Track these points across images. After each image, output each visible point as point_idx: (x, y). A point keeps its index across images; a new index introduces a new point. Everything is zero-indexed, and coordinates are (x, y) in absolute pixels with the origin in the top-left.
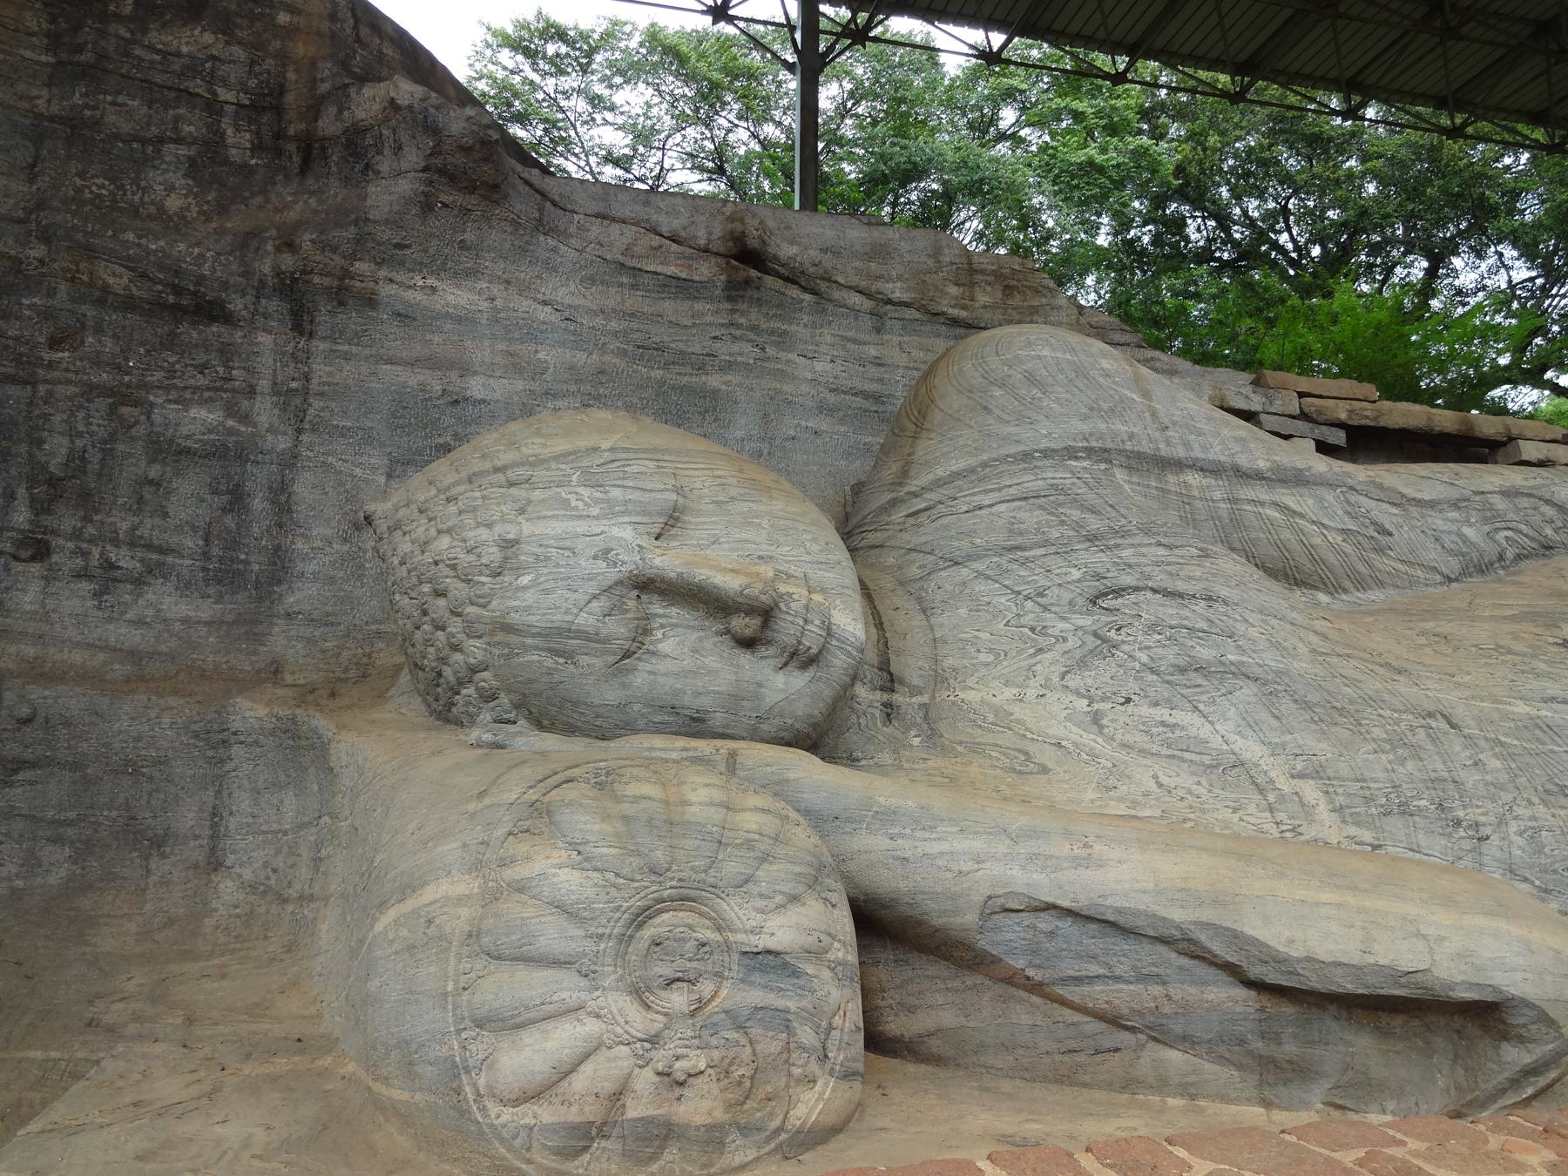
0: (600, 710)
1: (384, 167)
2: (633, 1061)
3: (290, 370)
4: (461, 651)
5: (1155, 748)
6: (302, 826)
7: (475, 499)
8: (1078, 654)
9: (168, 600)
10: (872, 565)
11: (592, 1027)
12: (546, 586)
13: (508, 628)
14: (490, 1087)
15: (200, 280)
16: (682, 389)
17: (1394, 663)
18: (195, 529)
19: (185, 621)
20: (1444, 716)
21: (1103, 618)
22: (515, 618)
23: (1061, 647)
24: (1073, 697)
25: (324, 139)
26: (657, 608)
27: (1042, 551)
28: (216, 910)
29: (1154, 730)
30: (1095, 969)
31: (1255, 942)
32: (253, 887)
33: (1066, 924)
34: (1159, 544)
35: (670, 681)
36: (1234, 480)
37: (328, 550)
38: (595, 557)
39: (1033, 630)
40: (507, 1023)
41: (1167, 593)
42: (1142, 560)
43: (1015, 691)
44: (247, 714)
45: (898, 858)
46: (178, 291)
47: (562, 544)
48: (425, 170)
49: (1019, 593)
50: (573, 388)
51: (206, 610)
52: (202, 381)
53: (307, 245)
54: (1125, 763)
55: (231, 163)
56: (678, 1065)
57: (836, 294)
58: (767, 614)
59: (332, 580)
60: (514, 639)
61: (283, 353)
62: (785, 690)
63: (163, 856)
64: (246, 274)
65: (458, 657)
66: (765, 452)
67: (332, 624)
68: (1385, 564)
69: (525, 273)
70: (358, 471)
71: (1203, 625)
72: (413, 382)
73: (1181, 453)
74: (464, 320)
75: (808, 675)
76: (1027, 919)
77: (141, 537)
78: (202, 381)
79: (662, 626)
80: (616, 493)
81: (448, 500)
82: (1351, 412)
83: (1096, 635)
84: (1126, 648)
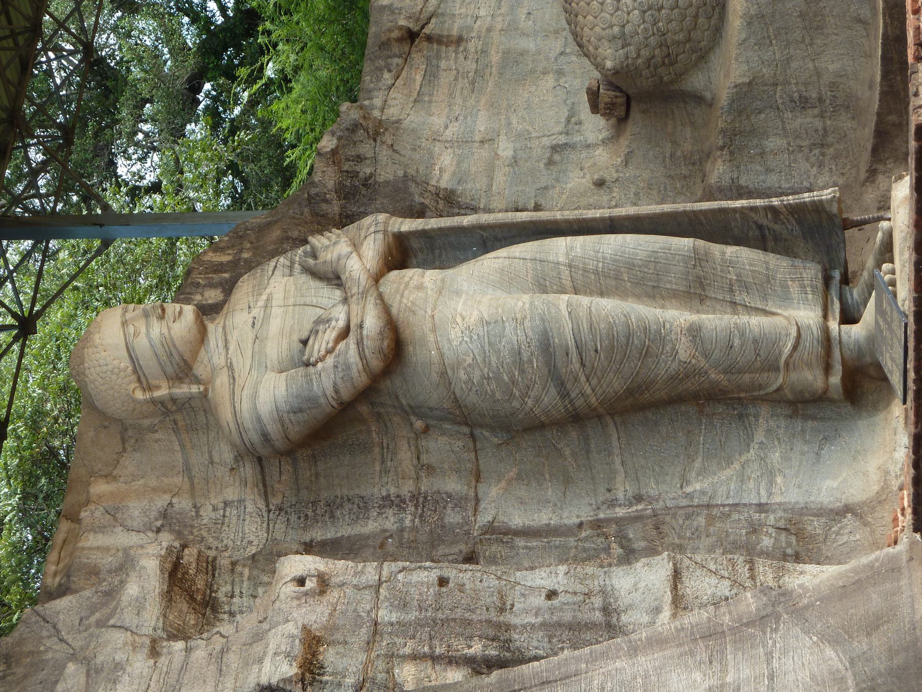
1: (368, 171)
25: (340, 215)
32: (821, 165)
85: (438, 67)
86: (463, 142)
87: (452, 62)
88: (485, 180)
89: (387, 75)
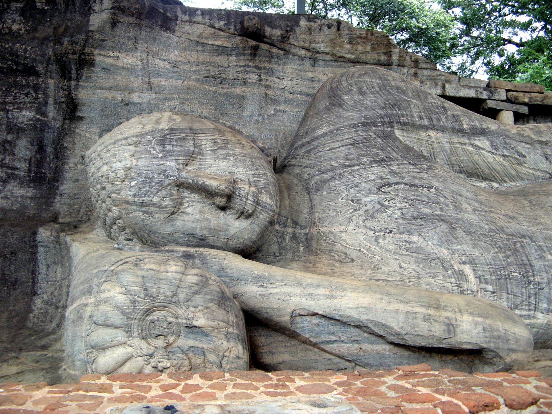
0: (164, 235)
2: (144, 362)
3: (61, 94)
4: (111, 211)
5: (401, 252)
6: (63, 279)
7: (116, 151)
8: (371, 212)
9: (15, 189)
10: (290, 174)
11: (129, 350)
12: (141, 186)
13: (128, 203)
14: (96, 369)
15: (26, 58)
16: (224, 95)
17: (510, 214)
18: (25, 160)
19: (22, 197)
20: (529, 237)
21: (383, 196)
22: (131, 198)
23: (364, 208)
24: (368, 230)
26: (186, 194)
27: (358, 167)
28: (34, 310)
29: (401, 244)
30: (333, 338)
31: (389, 327)
32: (47, 303)
33: (323, 320)
34: (410, 163)
35: (191, 224)
36: (452, 134)
37: (76, 168)
38: (160, 174)
39: (353, 201)
40: (102, 348)
41: (411, 185)
42: (402, 171)
43: (343, 227)
44: (43, 235)
45: (261, 295)
46: (17, 64)
47: (147, 169)
48: (112, 8)
49: (347, 186)
50: (177, 96)
51: (30, 192)
52: (28, 100)
53: (66, 43)
54: (387, 258)
55: (38, 9)
56: (160, 364)
57: (293, 50)
58: (229, 197)
59: (77, 180)
60: (130, 207)
61: (58, 87)
62: (239, 228)
63: (15, 289)
64: (43, 55)
65: (110, 214)
66: (261, 121)
67: (77, 198)
68: (523, 170)
69: (155, 48)
70: (88, 135)
71: (426, 199)
72: (110, 96)
73: (426, 122)
74: (130, 70)
75: (249, 221)
76: (308, 318)
77: (5, 164)
78: (28, 100)
79: (188, 202)
80: (168, 147)
81: (108, 151)
82: (530, 98)
83: (379, 203)
84: (391, 209)
85: (231, 55)
86: (147, 70)
87: (235, 64)
88: (108, 85)
89: (222, 23)
